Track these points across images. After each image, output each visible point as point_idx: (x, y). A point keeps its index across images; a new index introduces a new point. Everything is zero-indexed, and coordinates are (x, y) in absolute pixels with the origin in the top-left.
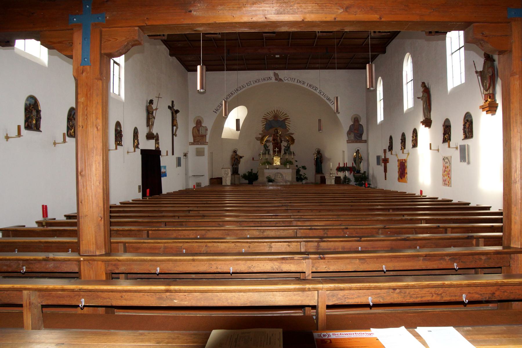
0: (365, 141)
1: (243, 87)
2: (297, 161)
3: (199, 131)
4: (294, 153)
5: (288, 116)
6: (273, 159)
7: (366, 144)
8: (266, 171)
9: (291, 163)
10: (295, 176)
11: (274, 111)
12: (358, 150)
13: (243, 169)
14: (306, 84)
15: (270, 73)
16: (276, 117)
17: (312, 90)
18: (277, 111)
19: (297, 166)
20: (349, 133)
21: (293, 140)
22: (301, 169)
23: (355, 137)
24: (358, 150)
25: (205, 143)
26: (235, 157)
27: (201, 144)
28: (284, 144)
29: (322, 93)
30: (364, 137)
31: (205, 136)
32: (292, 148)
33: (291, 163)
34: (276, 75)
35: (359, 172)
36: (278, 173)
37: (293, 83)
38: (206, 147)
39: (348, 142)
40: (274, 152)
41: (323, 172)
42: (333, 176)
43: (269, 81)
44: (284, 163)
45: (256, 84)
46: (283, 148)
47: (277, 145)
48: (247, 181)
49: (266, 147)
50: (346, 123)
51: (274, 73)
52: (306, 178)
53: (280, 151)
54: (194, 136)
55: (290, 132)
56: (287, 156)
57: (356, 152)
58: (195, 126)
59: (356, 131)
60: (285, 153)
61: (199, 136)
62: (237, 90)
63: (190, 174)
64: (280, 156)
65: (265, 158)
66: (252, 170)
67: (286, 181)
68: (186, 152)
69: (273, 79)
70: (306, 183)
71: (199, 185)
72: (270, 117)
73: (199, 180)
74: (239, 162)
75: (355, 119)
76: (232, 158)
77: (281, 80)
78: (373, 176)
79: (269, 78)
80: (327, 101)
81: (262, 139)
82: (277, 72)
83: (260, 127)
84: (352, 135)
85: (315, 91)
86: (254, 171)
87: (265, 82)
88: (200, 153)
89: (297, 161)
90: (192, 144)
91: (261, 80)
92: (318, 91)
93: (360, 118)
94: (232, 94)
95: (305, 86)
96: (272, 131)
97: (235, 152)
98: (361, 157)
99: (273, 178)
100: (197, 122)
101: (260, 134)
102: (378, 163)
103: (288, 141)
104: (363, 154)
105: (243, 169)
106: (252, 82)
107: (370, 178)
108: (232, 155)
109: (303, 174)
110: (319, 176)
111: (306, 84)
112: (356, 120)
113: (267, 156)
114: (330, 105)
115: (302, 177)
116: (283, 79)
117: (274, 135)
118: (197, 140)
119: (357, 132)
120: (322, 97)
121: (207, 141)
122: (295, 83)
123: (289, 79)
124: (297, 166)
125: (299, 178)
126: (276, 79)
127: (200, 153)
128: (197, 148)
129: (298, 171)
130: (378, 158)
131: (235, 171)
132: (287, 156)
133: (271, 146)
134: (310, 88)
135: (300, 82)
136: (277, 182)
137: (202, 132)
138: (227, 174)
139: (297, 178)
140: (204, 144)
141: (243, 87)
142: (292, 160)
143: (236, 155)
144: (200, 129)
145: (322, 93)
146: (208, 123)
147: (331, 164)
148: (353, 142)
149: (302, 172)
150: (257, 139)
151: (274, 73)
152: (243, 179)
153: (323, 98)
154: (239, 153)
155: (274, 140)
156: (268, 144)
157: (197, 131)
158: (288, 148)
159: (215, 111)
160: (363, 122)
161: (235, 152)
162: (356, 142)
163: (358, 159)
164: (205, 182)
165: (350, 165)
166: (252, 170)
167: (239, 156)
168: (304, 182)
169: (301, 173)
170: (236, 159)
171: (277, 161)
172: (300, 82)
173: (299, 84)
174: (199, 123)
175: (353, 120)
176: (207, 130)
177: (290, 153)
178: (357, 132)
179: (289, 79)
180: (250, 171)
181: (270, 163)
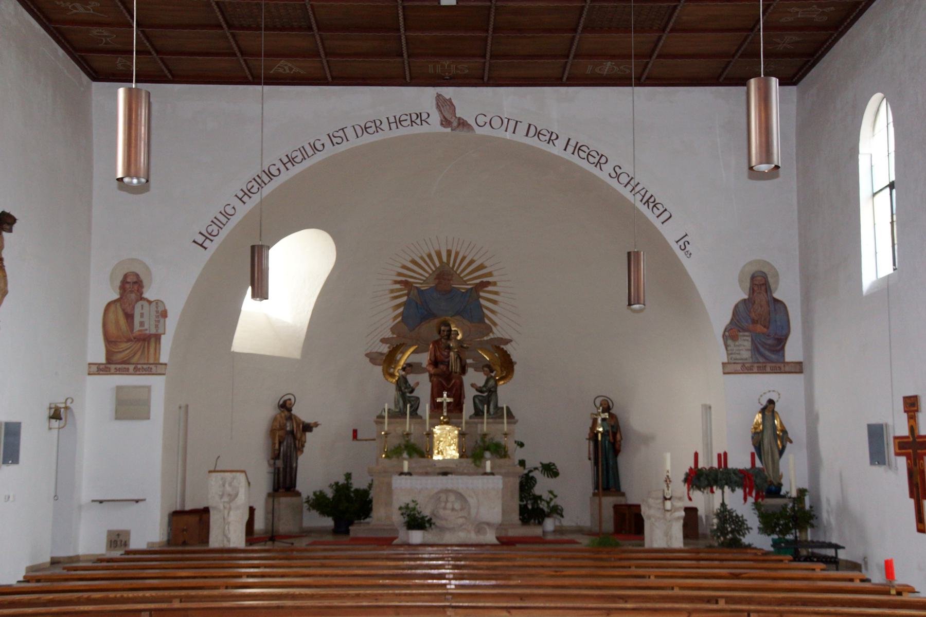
0: (798, 368)
1: (314, 148)
2: (521, 445)
3: (129, 317)
4: (510, 415)
5: (490, 274)
6: (430, 434)
7: (801, 376)
8: (399, 482)
9: (499, 451)
10: (515, 504)
11: (439, 254)
12: (771, 402)
13: (315, 472)
14: (560, 143)
15: (422, 98)
16: (444, 275)
17: (584, 164)
18: (449, 253)
19: (522, 463)
20: (731, 333)
21: (507, 365)
22: (537, 474)
23: (755, 349)
24: (771, 402)
25: (152, 367)
26: (283, 428)
27: (137, 372)
28: (473, 379)
29: (624, 179)
30: (793, 351)
31: (158, 337)
32: (505, 393)
33: (499, 451)
34: (443, 104)
35: (774, 490)
36: (447, 491)
37: (508, 135)
38: (157, 385)
39: (728, 369)
40: (436, 407)
41: (624, 487)
42: (674, 509)
43: (417, 129)
44: (475, 451)
45: (366, 139)
46: (470, 394)
47: (446, 380)
48: (329, 522)
49: (404, 389)
50: (720, 298)
51: (439, 96)
52: (556, 511)
53: (457, 407)
54: (109, 341)
55: (497, 333)
56: (485, 426)
57: (763, 411)
58: (116, 296)
59: (760, 328)
60: (478, 413)
61: (129, 340)
62: (292, 160)
63: (86, 493)
64: (457, 425)
65: (399, 430)
66: (348, 476)
67: (480, 527)
68: (60, 401)
69: (435, 118)
70: (559, 531)
71: (117, 539)
72: (422, 277)
73: (119, 520)
74: (298, 446)
75: (753, 278)
76: (272, 432)
77: (463, 124)
78: (843, 510)
79: (419, 116)
80: (643, 209)
81: (389, 360)
82: (448, 92)
83: (381, 316)
84: (745, 344)
85: (596, 171)
86: (359, 483)
87: (402, 131)
88: (129, 408)
89: (521, 445)
90: (101, 370)
91: (385, 126)
92: (608, 168)
93: (776, 275)
94: (270, 175)
95: (557, 150)
96: (429, 330)
97: (285, 406)
98: (784, 431)
99: (426, 512)
100: (124, 282)
101: (384, 341)
102: (877, 456)
103: (488, 368)
104: (791, 417)
105: (315, 472)
106: (350, 132)
107: (827, 515)
108: (275, 419)
109: (546, 496)
110: (609, 502)
111: (560, 143)
112: (760, 283)
113: (408, 425)
114: (657, 223)
115: (543, 506)
116: (471, 122)
117: (436, 343)
118: (119, 356)
119: (762, 330)
120: (626, 192)
121: (164, 359)
122: (520, 137)
123: (496, 122)
124: (522, 463)
125: (532, 509)
126: (446, 122)
127: (129, 408)
128: (119, 389)
129: (526, 484)
130: (876, 433)
131: (284, 482)
132: (485, 426)
133: (423, 386)
134: (575, 159)
135: (538, 133)
136: (442, 529)
137: (144, 319)
138: (233, 497)
139: (523, 510)
140: (149, 372)
141: (314, 148)
142: (504, 441)
143: (291, 417)
144: (138, 306)
145: (624, 179)
146: (172, 289)
147: (668, 456)
148: (747, 370)
149: (543, 486)
150: (373, 358)
151: (439, 96)
152: (315, 513)
153: (630, 197)
154: (302, 412)
155: (435, 363)
156: (412, 379)
157: (122, 321)
158: (487, 395)
159: (200, 239)
160: (787, 291)
161: (285, 406)
162: (762, 370)
163: (770, 438)
164: (148, 530)
165: (740, 460)
166: (348, 476)
167: (299, 422)
168: (550, 524)
169: (538, 490)
170: (288, 436)
171: (446, 444)
172: (538, 133)
173: (533, 142)
174: (131, 286)
175: (748, 284)
176: (164, 314)
177: (498, 413)
178: (762, 330)
179: (496, 122)
180: (342, 481)
181: (419, 449)
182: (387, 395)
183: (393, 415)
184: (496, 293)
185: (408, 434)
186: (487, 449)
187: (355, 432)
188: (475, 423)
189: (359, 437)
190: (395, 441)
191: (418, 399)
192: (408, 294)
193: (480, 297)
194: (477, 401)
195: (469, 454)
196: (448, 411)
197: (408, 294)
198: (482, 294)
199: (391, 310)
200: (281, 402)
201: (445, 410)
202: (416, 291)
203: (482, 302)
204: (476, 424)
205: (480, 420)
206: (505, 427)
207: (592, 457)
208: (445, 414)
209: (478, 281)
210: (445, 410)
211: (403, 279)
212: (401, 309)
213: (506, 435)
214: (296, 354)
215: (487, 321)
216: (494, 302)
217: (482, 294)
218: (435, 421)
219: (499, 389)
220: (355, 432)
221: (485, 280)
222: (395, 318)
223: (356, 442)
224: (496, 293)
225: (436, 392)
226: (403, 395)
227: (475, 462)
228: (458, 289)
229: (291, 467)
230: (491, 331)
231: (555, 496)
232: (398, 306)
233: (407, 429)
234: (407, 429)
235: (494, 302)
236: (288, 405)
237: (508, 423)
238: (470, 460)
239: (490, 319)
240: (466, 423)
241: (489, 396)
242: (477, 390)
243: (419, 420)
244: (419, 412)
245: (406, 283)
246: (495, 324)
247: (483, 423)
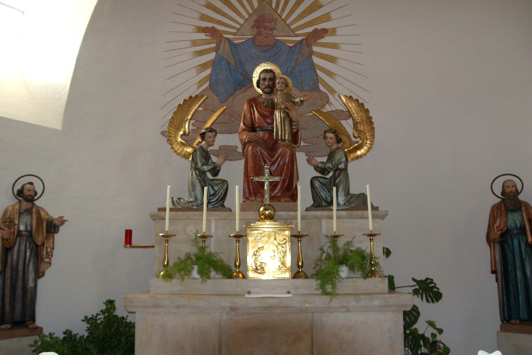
9: (364, 265)
32: (361, 176)
33: (364, 265)
40: (253, 191)
44: (324, 265)
46: (305, 172)
60: (321, 203)
64: (287, 222)
65: (191, 229)
113: (206, 222)
132: (334, 222)
133: (233, 173)
142: (365, 245)
158: (332, 175)
177: (357, 203)
181: (222, 265)
182: (175, 177)
183: (178, 207)
184: (335, 46)
185: (204, 237)
186: (343, 261)
187: (129, 234)
188: (316, 218)
189: (134, 242)
190: (182, 248)
191: (224, 182)
192: (216, 49)
193: (312, 53)
194: (317, 184)
195: (309, 270)
196: (272, 198)
197: (216, 49)
198: (315, 49)
199: (194, 72)
200: (18, 187)
201: (267, 196)
202: (227, 45)
203: (316, 60)
204: (319, 219)
205: (326, 213)
206: (371, 225)
207: (499, 268)
208: (267, 202)
209: (310, 29)
210: (267, 196)
211: (210, 25)
212: (208, 71)
213: (372, 235)
214: (54, 121)
215: (322, 88)
216: (332, 59)
217: (315, 49)
218: (250, 215)
219: (350, 165)
220: (129, 234)
221: (320, 27)
222: (201, 83)
223: (129, 251)
224: (335, 46)
225: (254, 169)
226: (201, 174)
227: (322, 287)
228: (283, 43)
229: (25, 289)
230: (328, 101)
231: (440, 331)
232: (204, 66)
233: (204, 230)
234: (204, 230)
235: (332, 59)
236: (26, 193)
237: (374, 217)
238: (313, 283)
239: (326, 85)
240: (303, 218)
241: (334, 177)
242: (316, 168)
243: (225, 214)
244: (227, 204)
245: (212, 32)
246: (333, 91)
247: (331, 217)
